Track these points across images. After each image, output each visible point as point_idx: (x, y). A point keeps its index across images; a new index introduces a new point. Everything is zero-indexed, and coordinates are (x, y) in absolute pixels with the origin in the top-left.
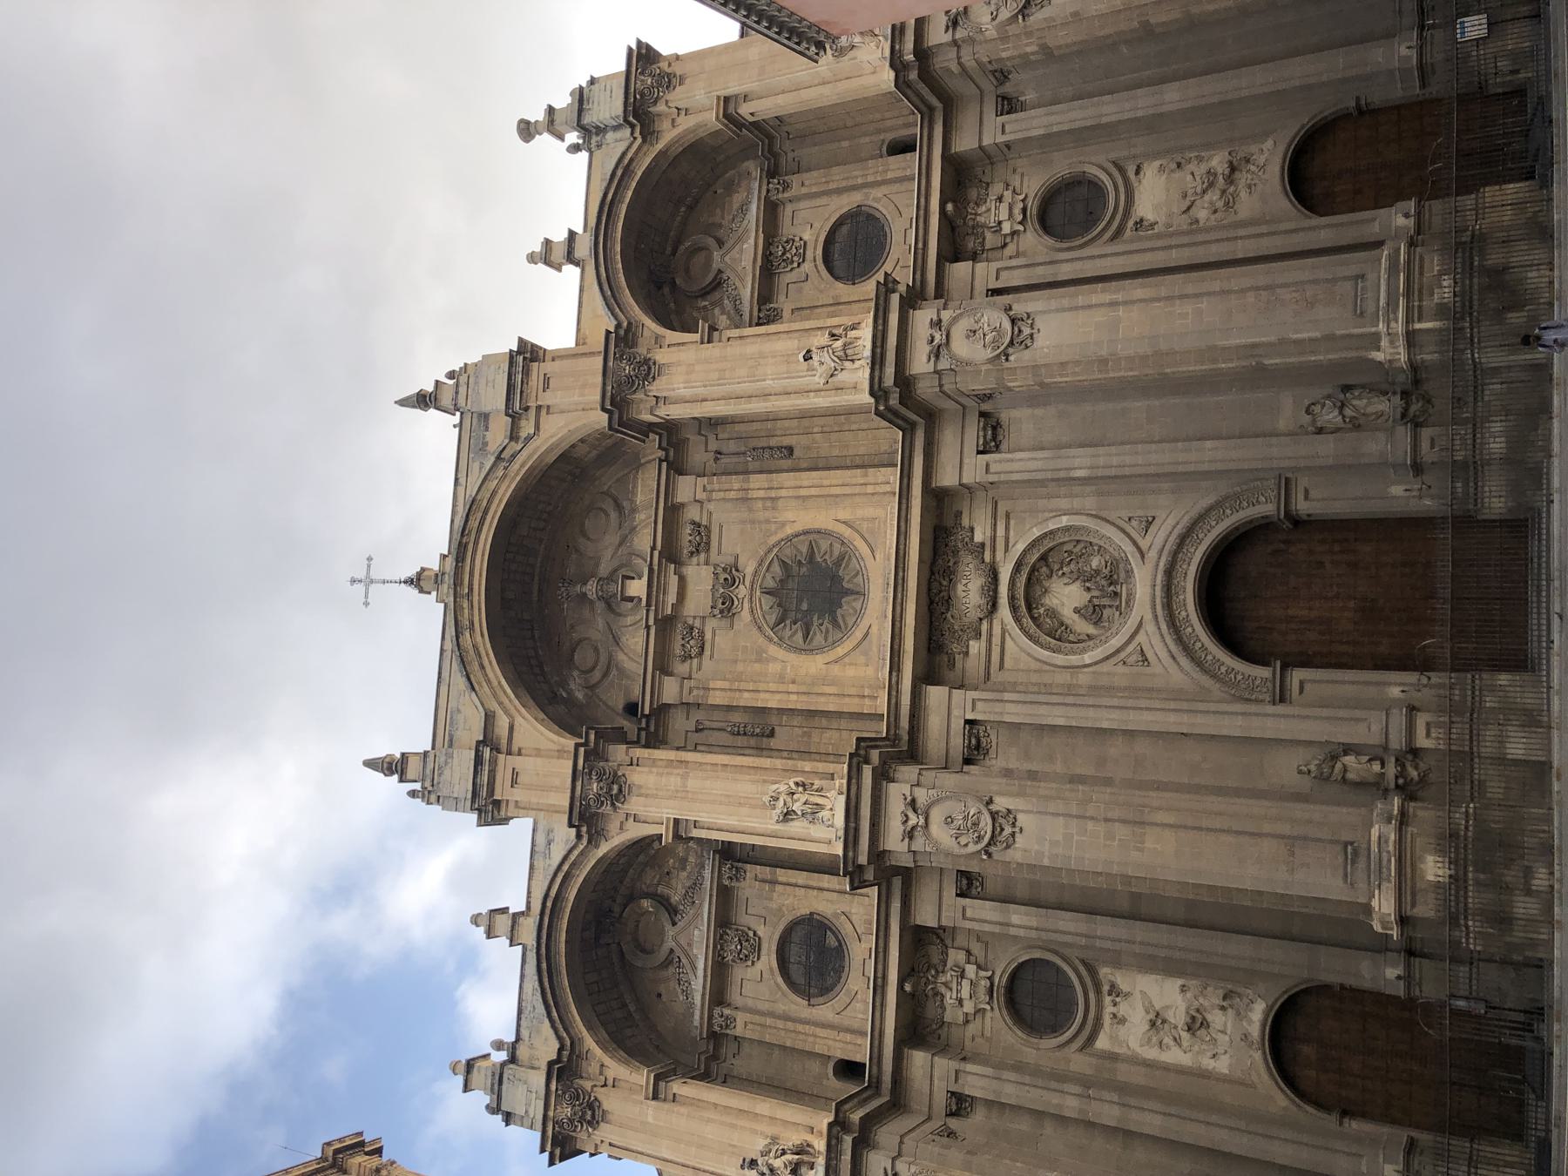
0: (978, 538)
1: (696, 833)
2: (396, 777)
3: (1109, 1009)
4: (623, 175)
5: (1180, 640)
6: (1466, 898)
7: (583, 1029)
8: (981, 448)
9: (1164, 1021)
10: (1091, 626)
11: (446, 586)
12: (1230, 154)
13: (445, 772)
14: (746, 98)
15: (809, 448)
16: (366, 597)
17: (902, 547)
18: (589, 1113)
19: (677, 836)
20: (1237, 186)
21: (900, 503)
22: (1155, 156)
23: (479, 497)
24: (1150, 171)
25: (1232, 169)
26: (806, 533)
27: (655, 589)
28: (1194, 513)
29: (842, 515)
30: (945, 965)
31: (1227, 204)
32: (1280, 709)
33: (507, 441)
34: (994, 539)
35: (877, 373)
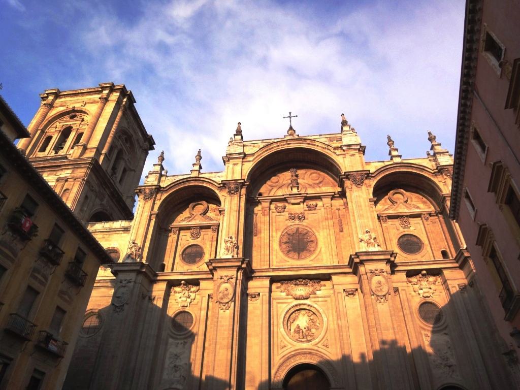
0: (318, 292)
1: (222, 216)
2: (235, 133)
3: (180, 342)
5: (289, 358)
7: (168, 194)
9: (177, 359)
12: (455, 365)
15: (343, 236)
18: (147, 197)
24: (446, 338)
25: (450, 366)
26: (317, 239)
34: (318, 297)
35: (363, 254)
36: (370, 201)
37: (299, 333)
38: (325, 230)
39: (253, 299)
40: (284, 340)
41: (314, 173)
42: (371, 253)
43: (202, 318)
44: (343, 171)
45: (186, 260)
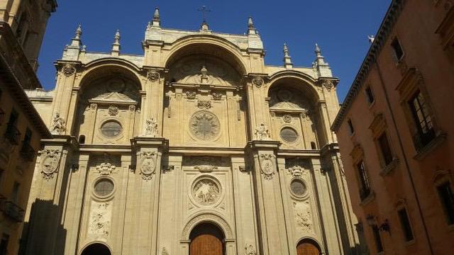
3: (102, 204)
14: (326, 108)
19: (142, 94)
22: (311, 207)
24: (307, 206)
25: (308, 226)
31: (299, 224)
34: (219, 171)
43: (123, 184)
44: (248, 72)
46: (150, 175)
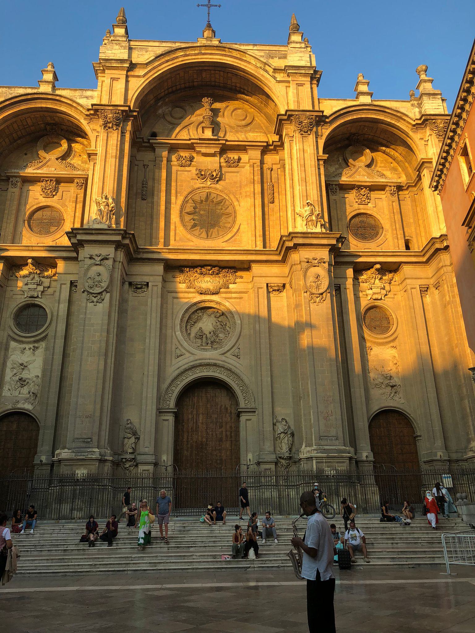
0: (231, 286)
1: (92, 163)
3: (27, 346)
4: (397, 116)
5: (186, 370)
6: (68, 486)
8: (269, 285)
9: (23, 369)
10: (194, 335)
11: (205, 42)
13: (117, 46)
15: (273, 211)
16: (202, 5)
17: (224, 252)
19: (89, 155)
20: (385, 388)
21: (244, 250)
23: (247, 55)
24: (393, 352)
25: (392, 387)
27: (207, 142)
28: (241, 374)
29: (242, 227)
30: (42, 278)
32: (154, 411)
33: (273, 67)
35: (299, 235)
36: (318, 160)
37: (202, 339)
38: (249, 199)
39: (140, 290)
40: (180, 347)
41: (239, 109)
42: (310, 235)
43: (61, 313)
45: (34, 229)
46: (100, 293)
